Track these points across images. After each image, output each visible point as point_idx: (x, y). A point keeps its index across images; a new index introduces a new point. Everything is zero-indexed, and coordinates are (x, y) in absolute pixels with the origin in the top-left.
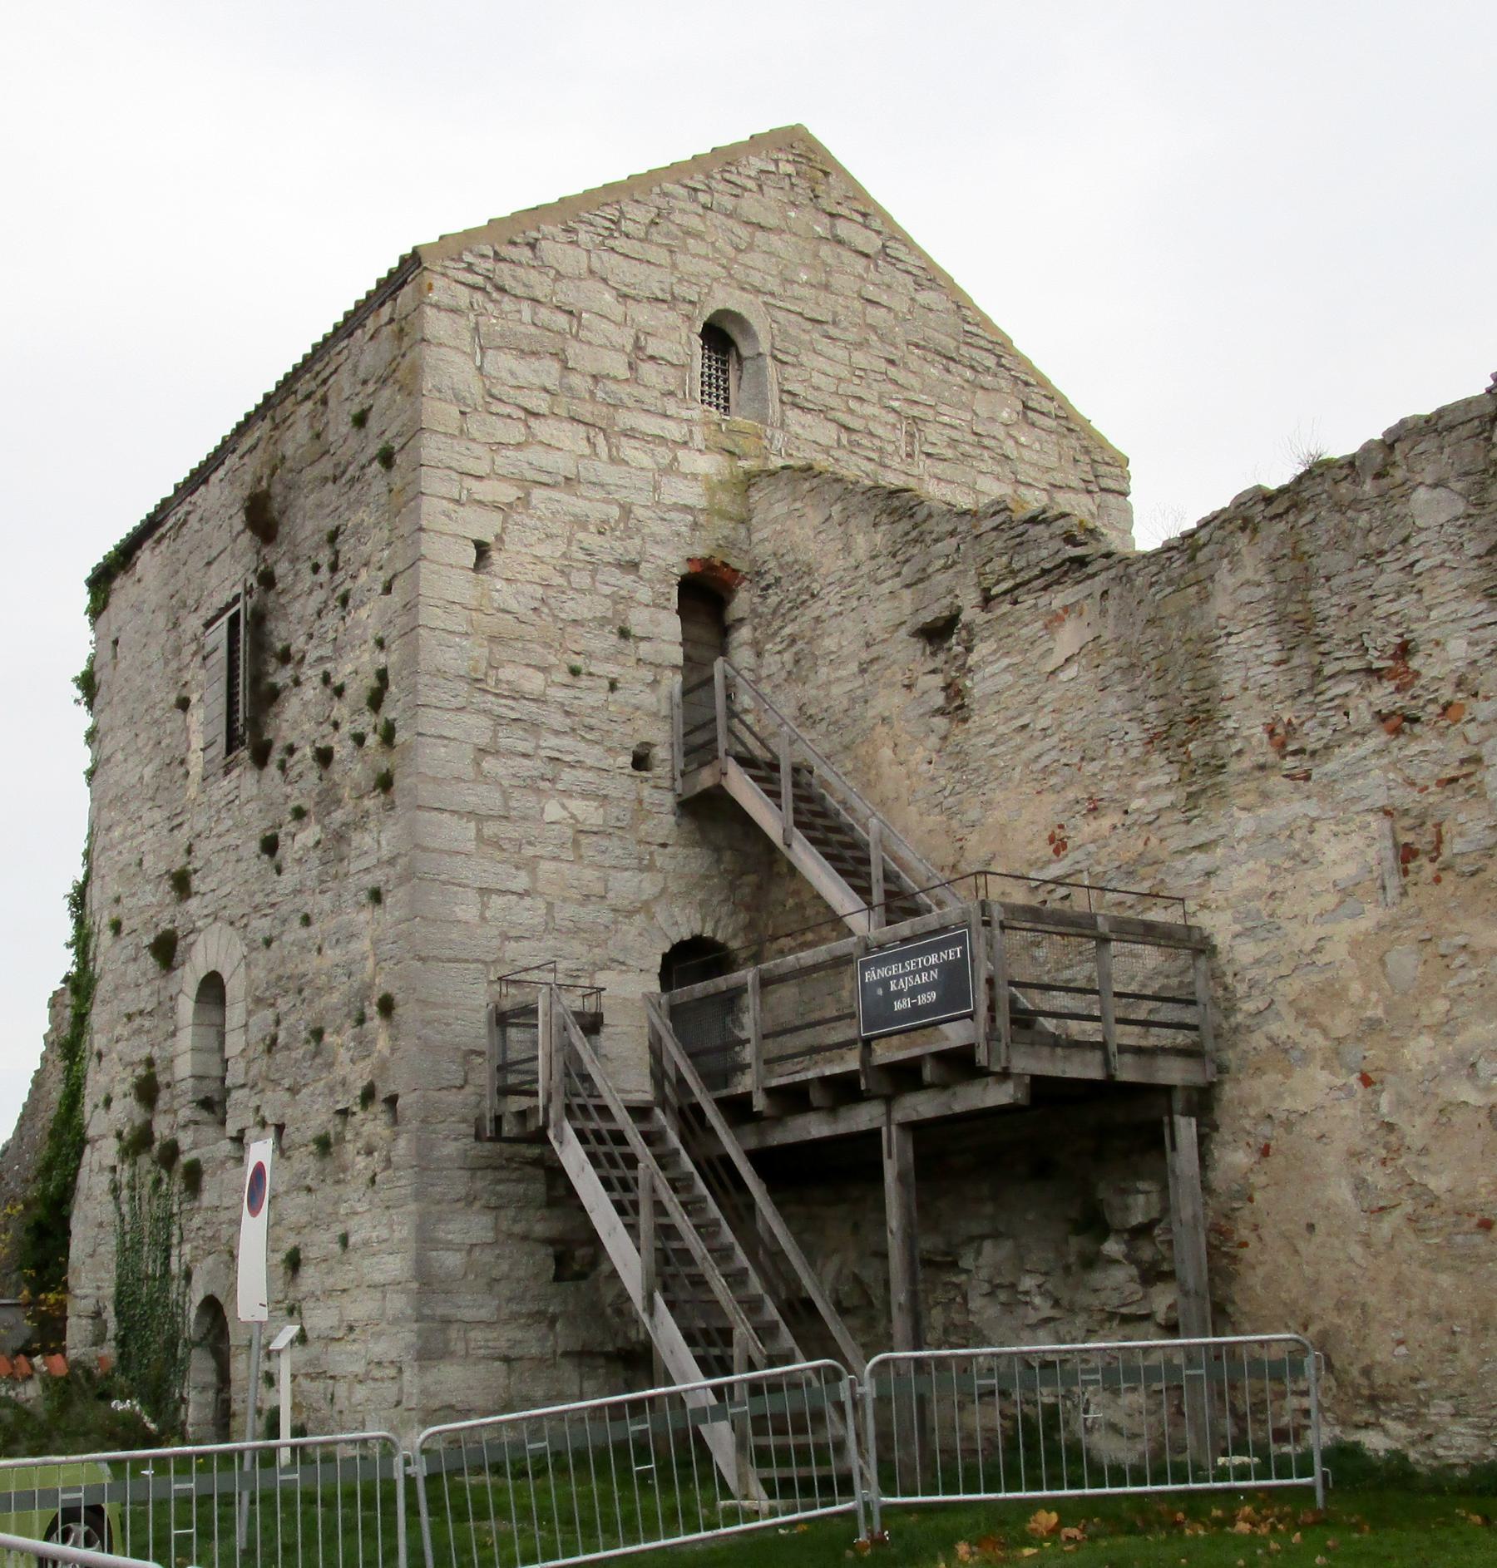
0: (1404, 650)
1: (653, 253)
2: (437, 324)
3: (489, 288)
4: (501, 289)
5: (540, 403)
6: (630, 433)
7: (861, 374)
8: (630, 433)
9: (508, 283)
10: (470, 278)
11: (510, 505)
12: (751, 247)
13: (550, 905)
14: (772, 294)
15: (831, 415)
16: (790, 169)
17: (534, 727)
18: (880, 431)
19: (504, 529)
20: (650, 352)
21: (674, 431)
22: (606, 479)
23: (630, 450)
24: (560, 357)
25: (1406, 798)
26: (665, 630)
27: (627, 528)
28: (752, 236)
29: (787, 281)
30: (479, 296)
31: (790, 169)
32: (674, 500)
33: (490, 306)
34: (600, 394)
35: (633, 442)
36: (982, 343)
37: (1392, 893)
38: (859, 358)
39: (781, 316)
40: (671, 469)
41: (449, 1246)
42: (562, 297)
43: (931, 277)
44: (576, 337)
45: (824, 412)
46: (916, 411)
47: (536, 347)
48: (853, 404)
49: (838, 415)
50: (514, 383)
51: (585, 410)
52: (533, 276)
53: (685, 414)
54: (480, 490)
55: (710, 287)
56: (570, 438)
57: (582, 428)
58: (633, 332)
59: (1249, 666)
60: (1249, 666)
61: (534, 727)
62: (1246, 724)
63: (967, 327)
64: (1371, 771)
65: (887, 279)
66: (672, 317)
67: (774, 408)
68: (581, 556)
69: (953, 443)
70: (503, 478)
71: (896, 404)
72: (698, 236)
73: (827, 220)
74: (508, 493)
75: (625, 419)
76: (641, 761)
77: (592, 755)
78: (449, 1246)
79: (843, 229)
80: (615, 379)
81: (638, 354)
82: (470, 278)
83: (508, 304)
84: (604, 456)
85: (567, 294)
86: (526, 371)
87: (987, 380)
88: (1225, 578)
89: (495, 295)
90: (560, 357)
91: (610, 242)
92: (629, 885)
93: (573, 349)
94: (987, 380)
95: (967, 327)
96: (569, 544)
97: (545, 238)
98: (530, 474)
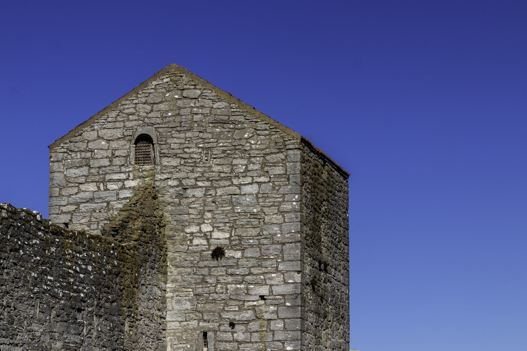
1: (118, 125)
3: (68, 151)
4: (71, 151)
5: (82, 180)
6: (110, 181)
7: (190, 140)
8: (110, 181)
9: (73, 148)
10: (62, 150)
11: (74, 211)
12: (152, 111)
14: (158, 124)
15: (178, 155)
16: (167, 80)
18: (195, 156)
19: (72, 218)
20: (116, 155)
21: (123, 176)
22: (102, 196)
24: (88, 165)
27: (108, 208)
28: (152, 108)
29: (163, 118)
30: (66, 155)
31: (167, 80)
32: (123, 196)
33: (69, 157)
34: (100, 172)
35: (111, 183)
36: (238, 114)
38: (189, 134)
40: (123, 188)
42: (90, 147)
44: (93, 158)
45: (175, 155)
46: (209, 145)
47: (81, 165)
48: (186, 150)
49: (181, 155)
50: (75, 176)
51: (97, 178)
53: (127, 170)
54: (64, 209)
55: (136, 129)
56: (92, 187)
57: (95, 184)
58: (110, 151)
63: (232, 110)
65: (202, 104)
66: (122, 142)
68: (95, 220)
69: (224, 152)
70: (71, 204)
71: (201, 146)
72: (133, 114)
73: (179, 92)
74: (72, 208)
75: (108, 177)
80: (105, 167)
82: (62, 150)
83: (73, 155)
84: (102, 189)
86: (77, 171)
89: (70, 153)
90: (88, 165)
91: (104, 126)
93: (92, 162)
95: (232, 110)
96: (91, 217)
97: (84, 132)
98: (79, 201)
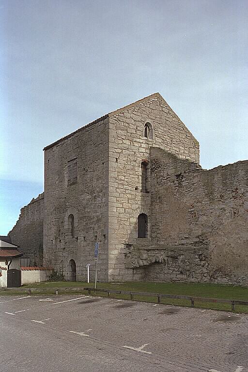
0: (237, 189)
2: (111, 126)
13: (125, 209)
16: (156, 100)
17: (123, 184)
21: (141, 141)
23: (135, 144)
25: (235, 207)
26: (140, 170)
31: (156, 100)
37: (233, 218)
39: (155, 123)
41: (113, 254)
43: (175, 116)
51: (130, 138)
52: (123, 118)
56: (128, 142)
59: (218, 186)
60: (218, 186)
61: (123, 184)
62: (217, 195)
64: (232, 203)
67: (154, 137)
75: (135, 140)
76: (136, 189)
77: (130, 188)
78: (113, 254)
79: (164, 109)
81: (136, 130)
85: (128, 121)
86: (123, 133)
87: (182, 132)
88: (216, 176)
92: (135, 206)
94: (182, 132)
